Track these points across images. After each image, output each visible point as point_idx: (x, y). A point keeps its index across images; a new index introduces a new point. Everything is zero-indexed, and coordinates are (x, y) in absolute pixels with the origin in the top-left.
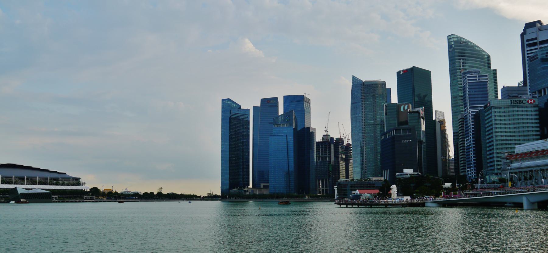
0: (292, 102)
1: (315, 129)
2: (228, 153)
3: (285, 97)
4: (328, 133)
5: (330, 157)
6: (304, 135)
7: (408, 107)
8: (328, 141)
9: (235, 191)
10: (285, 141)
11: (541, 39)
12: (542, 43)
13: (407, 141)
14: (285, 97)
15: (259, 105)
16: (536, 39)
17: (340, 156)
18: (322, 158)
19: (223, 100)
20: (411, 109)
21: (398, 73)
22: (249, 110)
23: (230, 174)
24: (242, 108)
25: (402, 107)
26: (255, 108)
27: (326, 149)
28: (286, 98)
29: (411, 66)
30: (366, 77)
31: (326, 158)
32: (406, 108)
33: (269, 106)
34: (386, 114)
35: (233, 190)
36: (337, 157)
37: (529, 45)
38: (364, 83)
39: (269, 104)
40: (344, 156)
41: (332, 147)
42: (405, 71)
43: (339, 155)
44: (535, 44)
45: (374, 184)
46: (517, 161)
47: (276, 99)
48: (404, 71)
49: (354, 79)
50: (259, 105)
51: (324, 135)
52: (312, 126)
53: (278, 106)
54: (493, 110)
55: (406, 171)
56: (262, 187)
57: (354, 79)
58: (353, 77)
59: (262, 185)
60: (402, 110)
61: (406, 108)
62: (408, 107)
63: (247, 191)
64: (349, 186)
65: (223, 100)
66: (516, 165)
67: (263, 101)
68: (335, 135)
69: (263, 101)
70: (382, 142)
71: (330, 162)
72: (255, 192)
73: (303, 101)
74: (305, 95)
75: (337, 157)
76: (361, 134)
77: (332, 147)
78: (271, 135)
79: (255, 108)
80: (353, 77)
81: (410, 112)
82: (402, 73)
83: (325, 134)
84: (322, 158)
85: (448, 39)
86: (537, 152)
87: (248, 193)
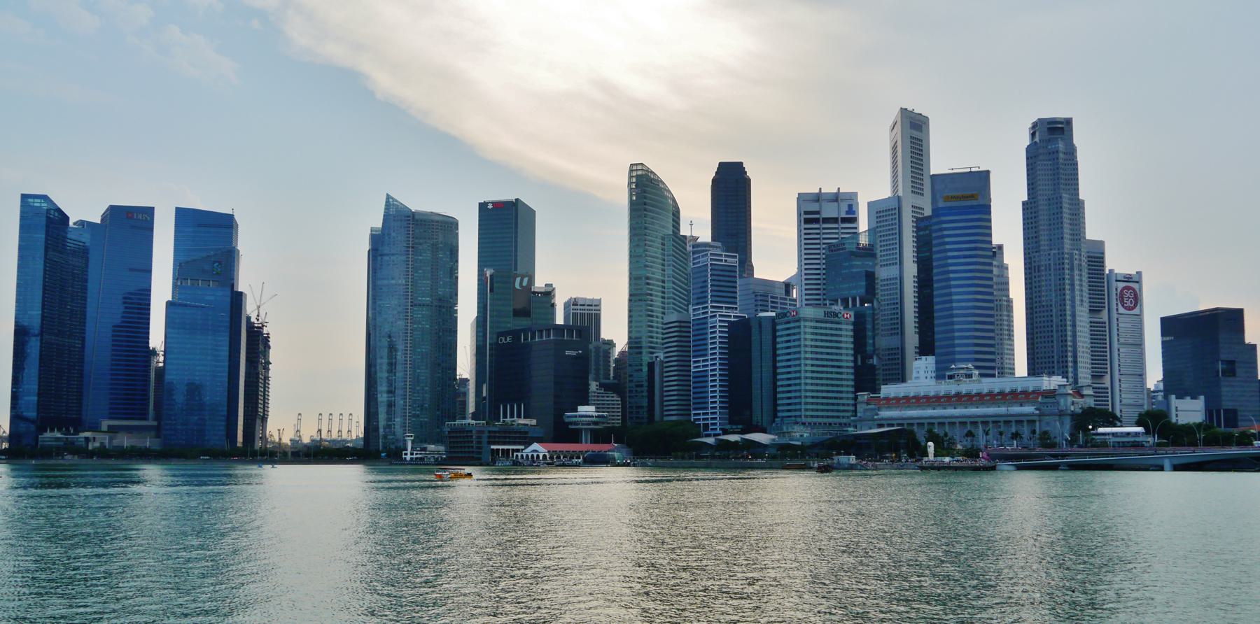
0: (199, 225)
9: (58, 439)
11: (825, 215)
12: (826, 220)
13: (574, 353)
16: (818, 213)
23: (39, 395)
25: (518, 280)
29: (512, 198)
30: (419, 202)
32: (525, 284)
37: (807, 221)
38: (414, 214)
42: (498, 205)
44: (816, 221)
45: (526, 433)
46: (889, 407)
47: (150, 211)
48: (496, 204)
49: (390, 202)
54: (802, 323)
55: (583, 409)
56: (104, 428)
57: (390, 202)
58: (388, 197)
60: (517, 286)
61: (525, 284)
64: (487, 434)
66: (885, 413)
70: (496, 347)
76: (401, 323)
80: (388, 197)
82: (490, 206)
85: (631, 171)
86: (927, 398)
87: (97, 444)
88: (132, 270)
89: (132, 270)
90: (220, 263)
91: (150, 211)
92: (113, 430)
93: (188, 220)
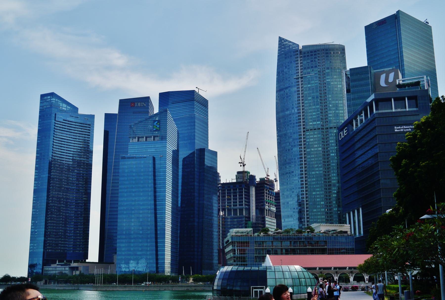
1: (215, 154)
2: (45, 194)
4: (246, 169)
5: (248, 210)
6: (197, 167)
7: (396, 77)
8: (245, 180)
10: (151, 169)
15: (115, 110)
17: (267, 207)
18: (235, 210)
19: (42, 96)
20: (400, 81)
21: (367, 28)
22: (92, 117)
24: (80, 112)
25: (383, 77)
26: (108, 117)
27: (241, 195)
31: (241, 210)
32: (391, 79)
34: (348, 91)
35: (53, 266)
36: (260, 209)
39: (133, 107)
40: (274, 209)
41: (253, 191)
43: (264, 205)
47: (146, 100)
49: (283, 44)
50: (115, 110)
51: (239, 173)
52: (212, 146)
58: (281, 40)
61: (391, 79)
62: (396, 77)
63: (77, 268)
65: (42, 96)
67: (123, 103)
68: (259, 176)
69: (123, 103)
71: (249, 218)
73: (193, 100)
74: (197, 90)
75: (260, 209)
77: (253, 191)
78: (124, 158)
79: (108, 117)
80: (281, 40)
81: (400, 86)
83: (241, 169)
84: (235, 210)
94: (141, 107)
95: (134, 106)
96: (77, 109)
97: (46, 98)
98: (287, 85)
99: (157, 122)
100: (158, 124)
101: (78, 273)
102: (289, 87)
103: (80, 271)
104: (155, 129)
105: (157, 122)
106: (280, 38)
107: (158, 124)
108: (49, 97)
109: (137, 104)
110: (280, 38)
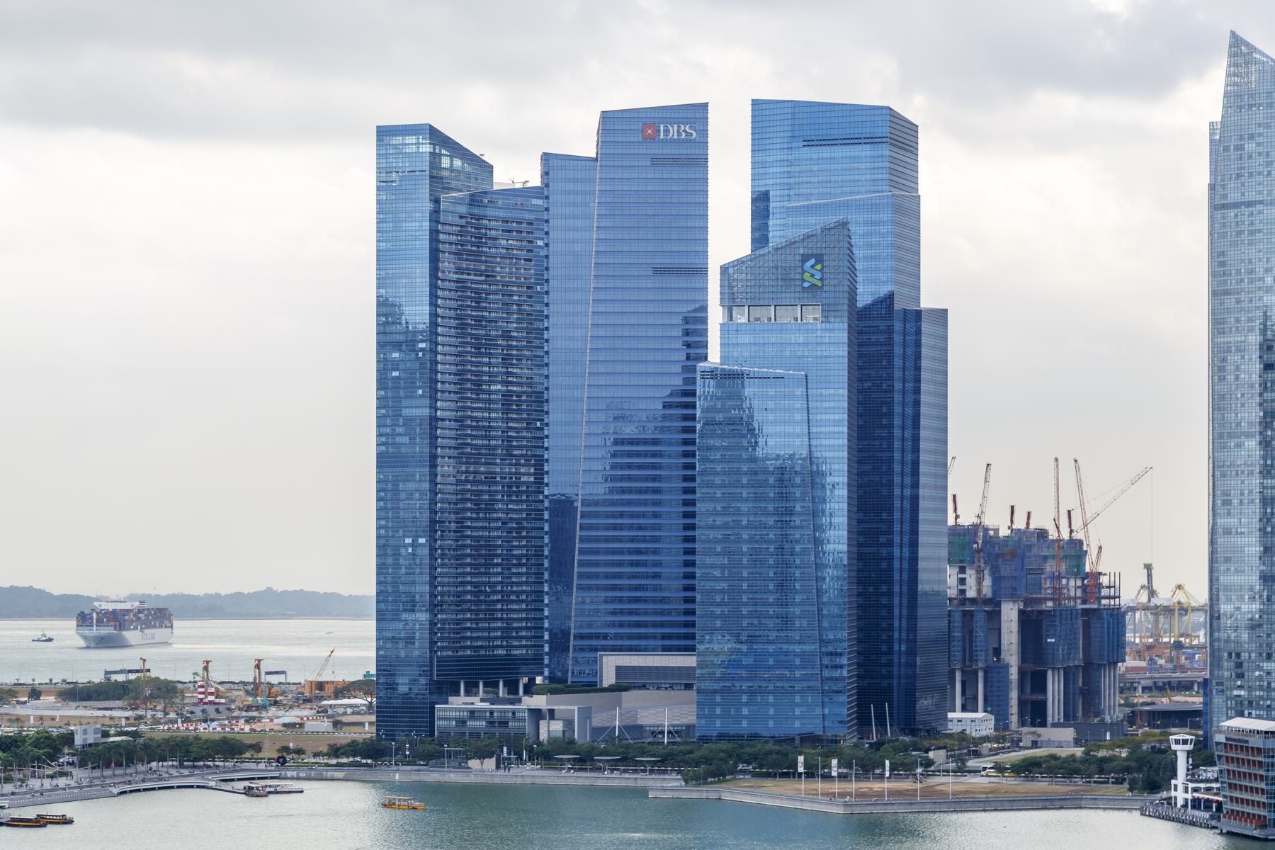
0: (809, 143)
3: (760, 109)
14: (760, 109)
15: (587, 147)
28: (766, 115)
33: (657, 161)
39: (659, 146)
47: (697, 114)
50: (587, 147)
53: (700, 161)
56: (609, 678)
59: (610, 666)
67: (610, 121)
69: (610, 121)
72: (599, 720)
87: (557, 727)
88: (659, 271)
89: (659, 271)
90: (819, 259)
91: (697, 114)
92: (629, 681)
93: (788, 128)
94: (679, 141)
95: (653, 139)
96: (489, 169)
97: (398, 140)
98: (1251, 196)
99: (812, 261)
100: (819, 267)
101: (557, 727)
102: (1261, 202)
103: (569, 723)
104: (806, 285)
105: (812, 261)
106: (1233, 34)
107: (819, 267)
108: (411, 139)
109: (666, 131)
110: (1233, 34)
